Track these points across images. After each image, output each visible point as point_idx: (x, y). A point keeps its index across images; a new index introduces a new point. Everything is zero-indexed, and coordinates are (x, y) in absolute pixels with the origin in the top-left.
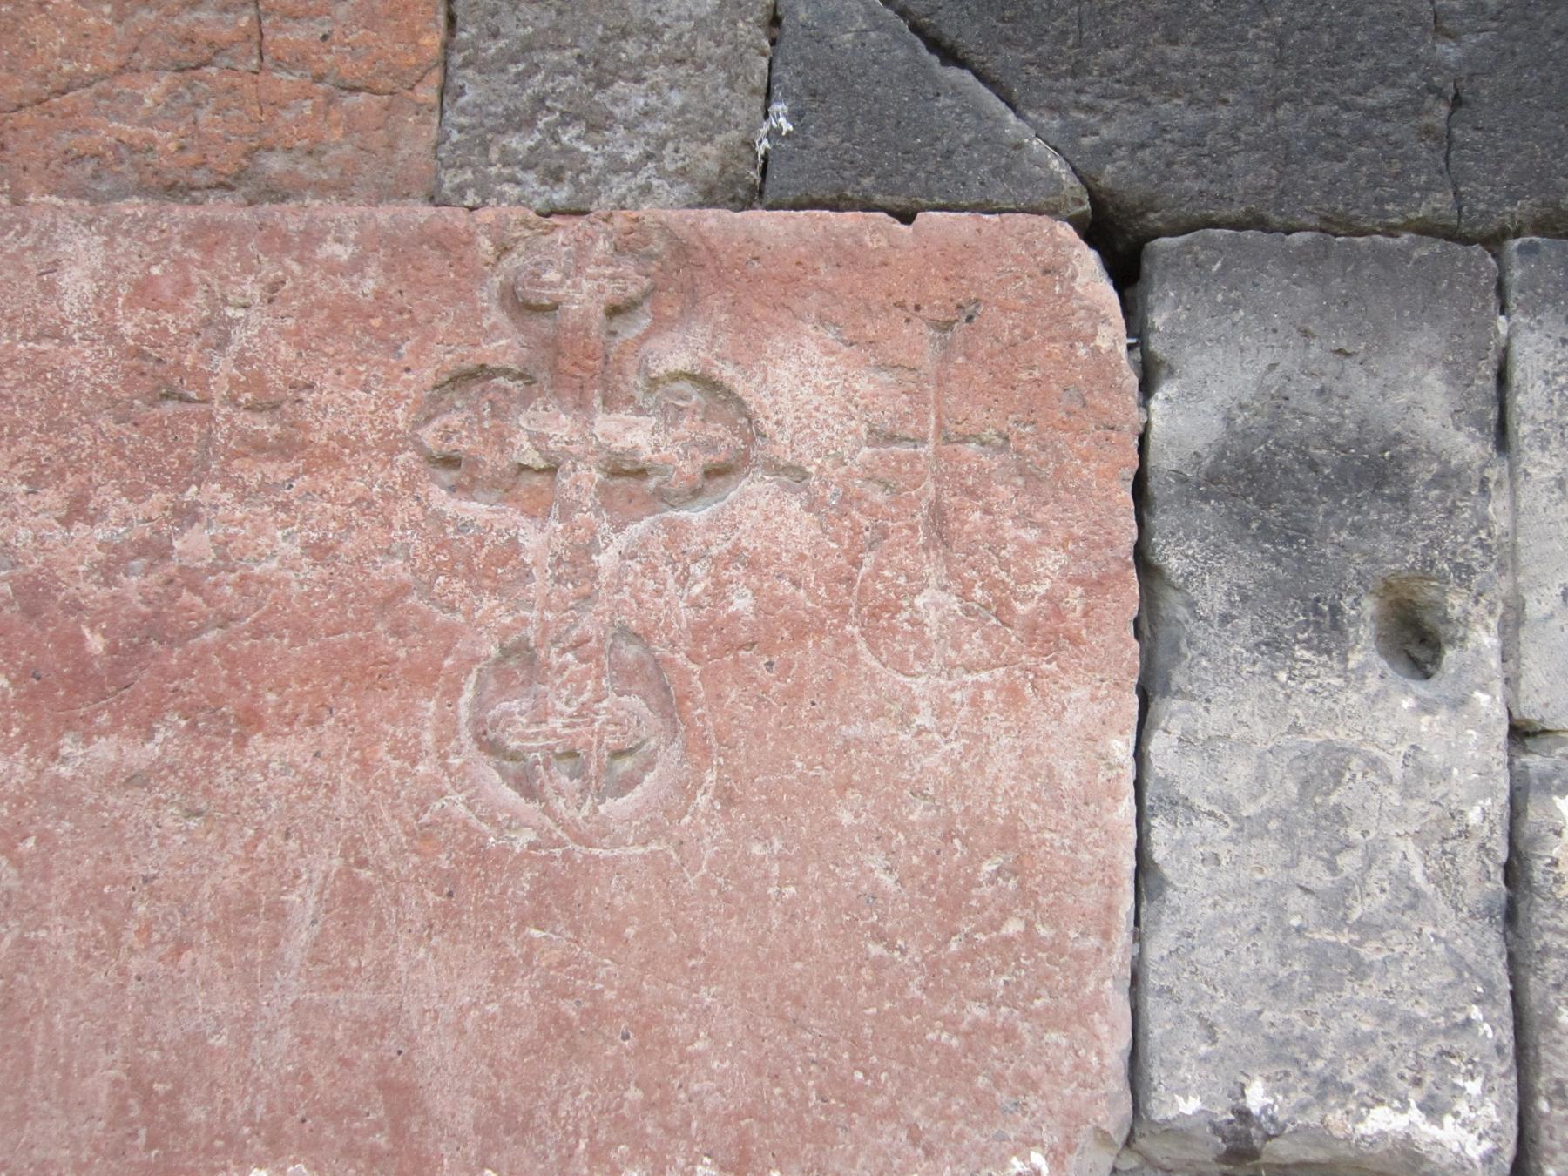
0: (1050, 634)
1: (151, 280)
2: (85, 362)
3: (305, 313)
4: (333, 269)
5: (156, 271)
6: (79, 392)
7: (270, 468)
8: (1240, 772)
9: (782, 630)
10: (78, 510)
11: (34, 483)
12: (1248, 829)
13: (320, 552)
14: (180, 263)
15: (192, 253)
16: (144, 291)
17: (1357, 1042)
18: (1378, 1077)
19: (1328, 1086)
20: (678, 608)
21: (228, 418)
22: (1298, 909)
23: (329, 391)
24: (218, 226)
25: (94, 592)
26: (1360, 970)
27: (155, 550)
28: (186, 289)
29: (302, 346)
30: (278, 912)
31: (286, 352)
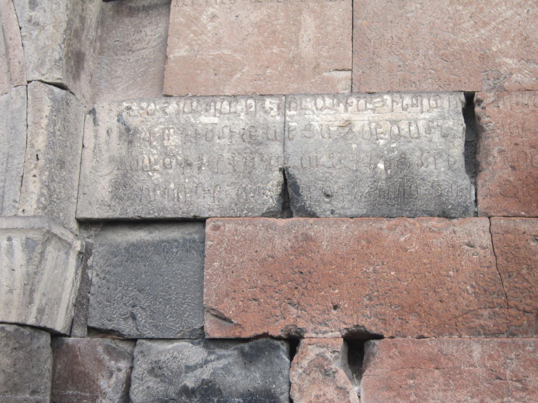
1: (492, 355)
2: (480, 371)
3: (525, 362)
4: (530, 352)
5: (492, 353)
6: (480, 378)
7: (521, 394)
11: (472, 397)
14: (498, 351)
15: (500, 349)
16: (490, 356)
21: (511, 383)
23: (531, 377)
24: (504, 343)
28: (499, 356)
29: (525, 369)
31: (522, 370)
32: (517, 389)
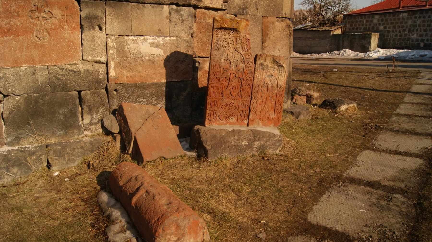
0: (74, 28)
4: (20, 3)
8: (88, 37)
9: (56, 29)
10: (2, 20)
12: (88, 41)
13: (22, 23)
16: (5, 4)
17: (96, 54)
18: (97, 56)
19: (94, 56)
20: (49, 27)
22: (92, 46)
25: (5, 26)
26: (96, 49)
27: (9, 23)
28: (8, 4)
30: (23, 48)
32: (16, 16)
